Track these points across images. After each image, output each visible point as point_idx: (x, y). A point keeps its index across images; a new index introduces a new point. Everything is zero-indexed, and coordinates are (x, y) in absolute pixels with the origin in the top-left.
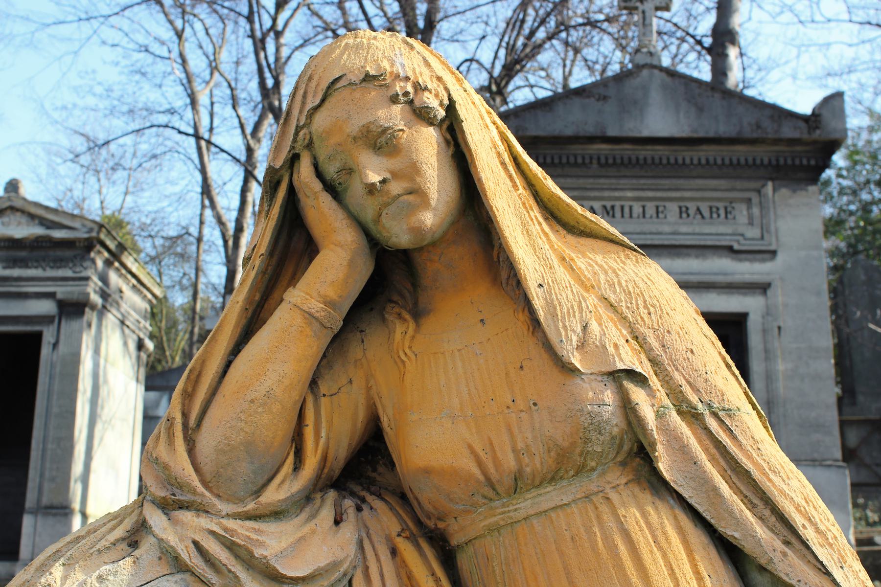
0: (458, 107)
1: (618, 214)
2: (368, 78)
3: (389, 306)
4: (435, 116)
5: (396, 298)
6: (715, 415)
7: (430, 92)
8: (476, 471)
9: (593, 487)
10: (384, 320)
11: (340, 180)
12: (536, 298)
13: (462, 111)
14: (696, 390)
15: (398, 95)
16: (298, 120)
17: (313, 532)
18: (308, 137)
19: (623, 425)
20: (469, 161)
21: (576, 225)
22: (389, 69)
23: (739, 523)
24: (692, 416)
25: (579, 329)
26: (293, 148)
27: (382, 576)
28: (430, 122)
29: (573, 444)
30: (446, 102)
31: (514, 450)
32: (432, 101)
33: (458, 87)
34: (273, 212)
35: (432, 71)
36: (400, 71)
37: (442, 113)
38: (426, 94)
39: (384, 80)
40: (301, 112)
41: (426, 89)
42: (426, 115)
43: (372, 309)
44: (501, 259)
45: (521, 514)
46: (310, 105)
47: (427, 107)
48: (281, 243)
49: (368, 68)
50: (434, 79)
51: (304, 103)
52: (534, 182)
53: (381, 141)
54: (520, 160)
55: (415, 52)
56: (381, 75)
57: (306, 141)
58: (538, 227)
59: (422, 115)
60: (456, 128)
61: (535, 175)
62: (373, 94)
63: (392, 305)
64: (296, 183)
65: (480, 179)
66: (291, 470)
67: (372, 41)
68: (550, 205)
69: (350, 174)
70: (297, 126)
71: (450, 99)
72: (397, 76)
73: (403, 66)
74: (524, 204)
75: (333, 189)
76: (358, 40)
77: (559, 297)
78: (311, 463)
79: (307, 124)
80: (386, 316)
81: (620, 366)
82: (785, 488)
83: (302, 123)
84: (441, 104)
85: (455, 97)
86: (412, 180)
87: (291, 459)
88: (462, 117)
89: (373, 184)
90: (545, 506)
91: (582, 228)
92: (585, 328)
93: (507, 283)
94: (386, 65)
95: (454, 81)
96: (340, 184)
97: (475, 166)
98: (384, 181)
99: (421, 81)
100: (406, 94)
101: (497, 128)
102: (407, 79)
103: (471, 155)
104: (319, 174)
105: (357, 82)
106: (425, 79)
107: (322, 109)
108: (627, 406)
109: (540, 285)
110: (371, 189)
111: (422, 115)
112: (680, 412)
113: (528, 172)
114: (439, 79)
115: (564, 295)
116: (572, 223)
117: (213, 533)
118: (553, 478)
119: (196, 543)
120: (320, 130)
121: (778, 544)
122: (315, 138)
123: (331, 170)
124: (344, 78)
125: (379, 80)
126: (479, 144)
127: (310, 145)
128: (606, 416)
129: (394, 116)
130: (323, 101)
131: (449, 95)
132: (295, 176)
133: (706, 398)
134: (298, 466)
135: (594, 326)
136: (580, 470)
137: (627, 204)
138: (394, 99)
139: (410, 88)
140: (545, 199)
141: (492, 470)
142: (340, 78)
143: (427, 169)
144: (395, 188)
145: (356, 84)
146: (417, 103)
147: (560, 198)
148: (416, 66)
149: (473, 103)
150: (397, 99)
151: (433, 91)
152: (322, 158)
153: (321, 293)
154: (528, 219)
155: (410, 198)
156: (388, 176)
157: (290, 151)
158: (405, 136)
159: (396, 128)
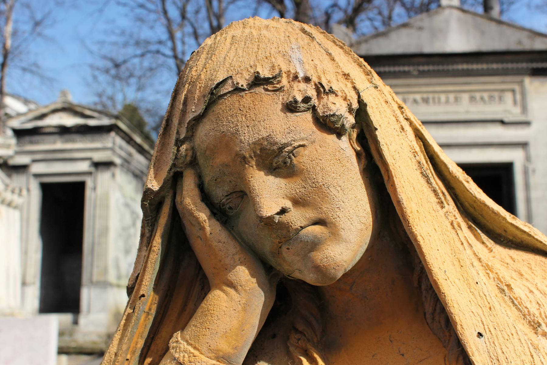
0: (369, 110)
1: (431, 101)
2: (258, 81)
3: (294, 337)
4: (343, 125)
5: (301, 327)
7: (337, 95)
10: (288, 353)
11: (231, 205)
12: (476, 353)
13: (375, 115)
15: (296, 102)
16: (178, 133)
18: (190, 153)
20: (385, 178)
21: (503, 233)
22: (284, 68)
26: (174, 165)
28: (339, 132)
30: (355, 106)
32: (338, 107)
33: (369, 85)
34: (155, 243)
35: (338, 67)
36: (299, 70)
37: (350, 120)
38: (332, 97)
39: (279, 82)
40: (180, 123)
41: (331, 91)
42: (332, 126)
43: (274, 336)
44: (423, 287)
46: (190, 116)
47: (334, 115)
48: (166, 275)
49: (259, 69)
50: (340, 77)
51: (184, 112)
52: (455, 185)
53: (277, 160)
54: (437, 159)
55: (315, 42)
56: (275, 78)
57: (189, 159)
58: (469, 251)
59: (327, 124)
60: (368, 136)
61: (456, 178)
63: (298, 336)
64: (179, 207)
65: (399, 202)
67: (264, 32)
68: (471, 210)
69: (242, 197)
70: (177, 140)
71: (360, 101)
73: (301, 62)
74: (452, 224)
75: (221, 213)
76: (247, 31)
77: (504, 347)
79: (189, 138)
80: (292, 349)
83: (182, 137)
84: (350, 110)
85: (366, 98)
88: (376, 124)
89: (271, 218)
91: (511, 238)
93: (433, 319)
95: (363, 77)
96: (230, 208)
97: (393, 185)
98: (283, 211)
99: (324, 83)
100: (307, 100)
101: (411, 124)
102: (307, 80)
103: (388, 170)
104: (206, 198)
105: (245, 87)
106: (331, 80)
107: (205, 120)
109: (480, 335)
110: (268, 222)
111: (327, 124)
113: (446, 174)
114: (346, 76)
115: (511, 349)
116: (498, 231)
120: (204, 146)
122: (198, 154)
123: (219, 193)
124: (230, 81)
125: (272, 83)
126: (397, 156)
127: (193, 163)
130: (207, 109)
131: (359, 96)
132: (178, 199)
137: (436, 96)
138: (291, 107)
139: (312, 92)
140: (467, 204)
142: (224, 81)
143: (335, 192)
145: (244, 90)
146: (320, 111)
147: (485, 205)
148: (316, 62)
149: (387, 102)
150: (296, 108)
151: (339, 93)
152: (207, 179)
153: (212, 348)
154: (459, 244)
155: (317, 229)
156: (288, 204)
157: (171, 169)
158: (306, 152)
159: (296, 144)
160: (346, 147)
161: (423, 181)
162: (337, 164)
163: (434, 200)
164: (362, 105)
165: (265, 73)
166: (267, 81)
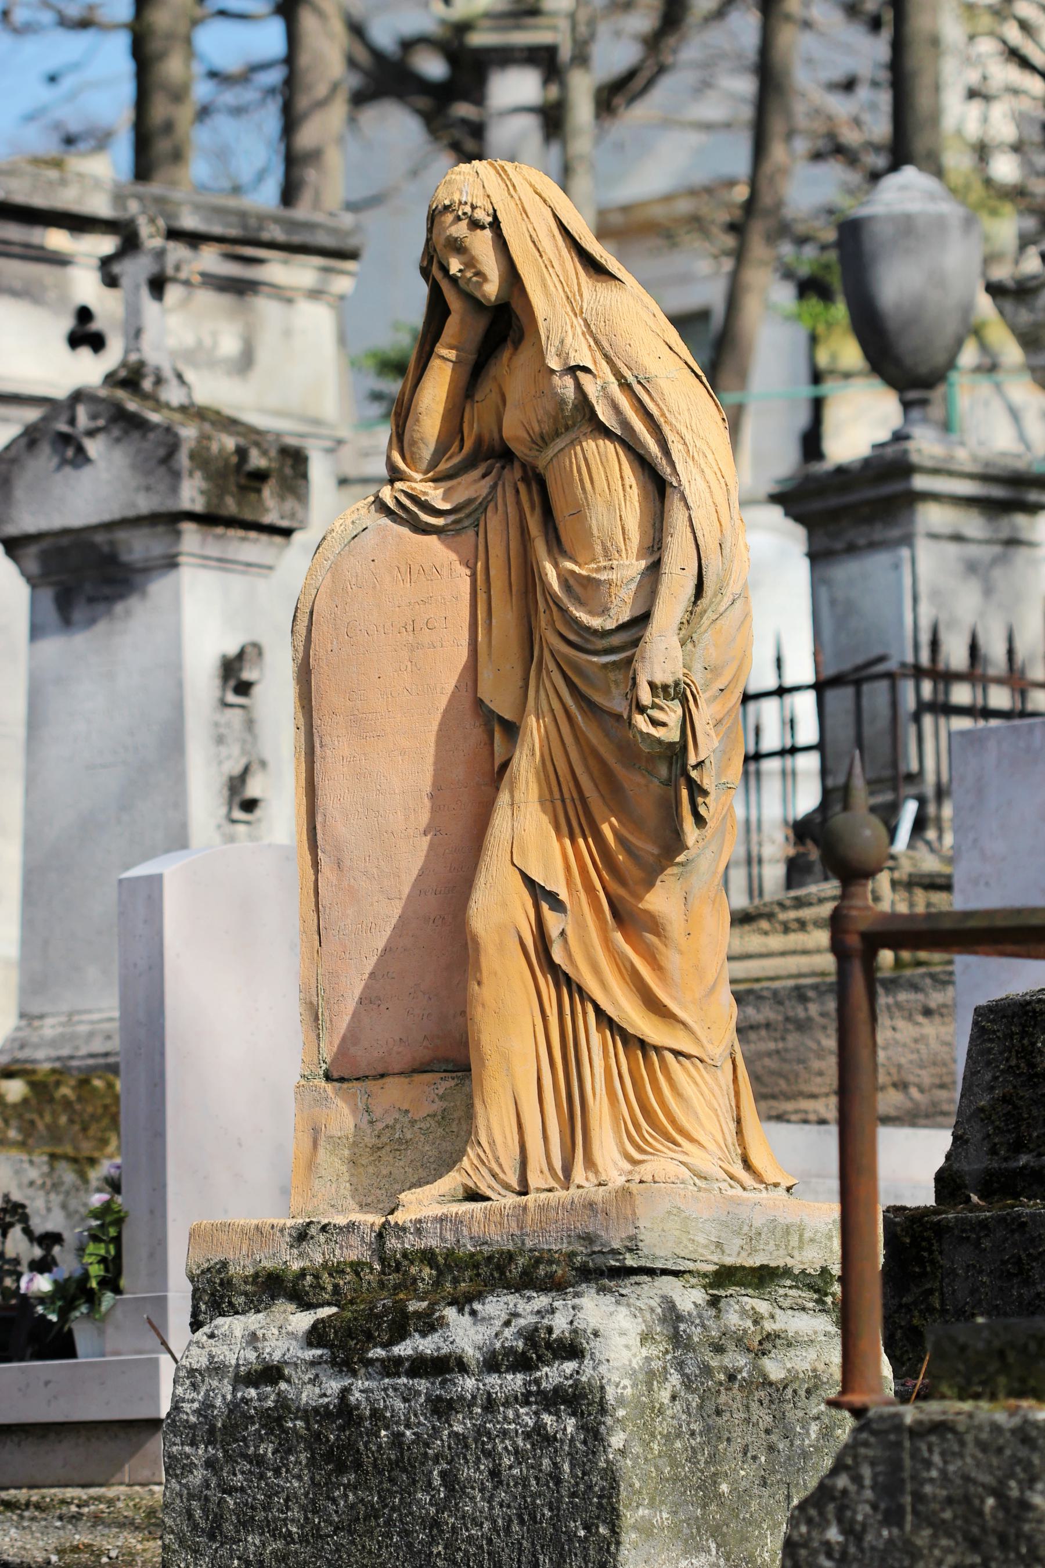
0: (498, 214)
2: (446, 208)
6: (639, 382)
8: (526, 435)
9: (574, 436)
14: (630, 369)
17: (459, 484)
19: (581, 398)
23: (643, 446)
24: (625, 386)
25: (557, 343)
27: (505, 505)
28: (483, 227)
29: (557, 413)
30: (491, 211)
31: (538, 421)
32: (480, 215)
38: (477, 211)
45: (549, 458)
59: (475, 225)
62: (449, 218)
66: (457, 449)
72: (460, 203)
78: (468, 444)
81: (572, 364)
82: (674, 422)
86: (474, 267)
87: (457, 443)
90: (556, 450)
92: (562, 342)
94: (456, 198)
98: (460, 271)
100: (465, 214)
108: (579, 387)
111: (475, 225)
112: (620, 385)
114: (488, 196)
117: (403, 491)
118: (557, 434)
119: (396, 498)
121: (659, 455)
128: (568, 394)
129: (460, 230)
133: (636, 373)
134: (461, 448)
135: (569, 340)
136: (567, 428)
138: (458, 219)
141: (531, 432)
144: (469, 274)
160: (488, 233)
161: (531, 245)
162: (482, 244)
163: (537, 254)
164: (495, 211)
165: (447, 202)
166: (449, 206)
